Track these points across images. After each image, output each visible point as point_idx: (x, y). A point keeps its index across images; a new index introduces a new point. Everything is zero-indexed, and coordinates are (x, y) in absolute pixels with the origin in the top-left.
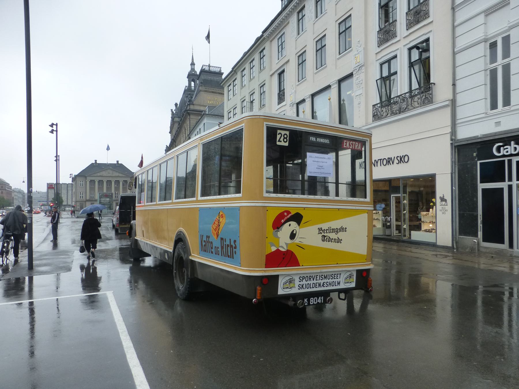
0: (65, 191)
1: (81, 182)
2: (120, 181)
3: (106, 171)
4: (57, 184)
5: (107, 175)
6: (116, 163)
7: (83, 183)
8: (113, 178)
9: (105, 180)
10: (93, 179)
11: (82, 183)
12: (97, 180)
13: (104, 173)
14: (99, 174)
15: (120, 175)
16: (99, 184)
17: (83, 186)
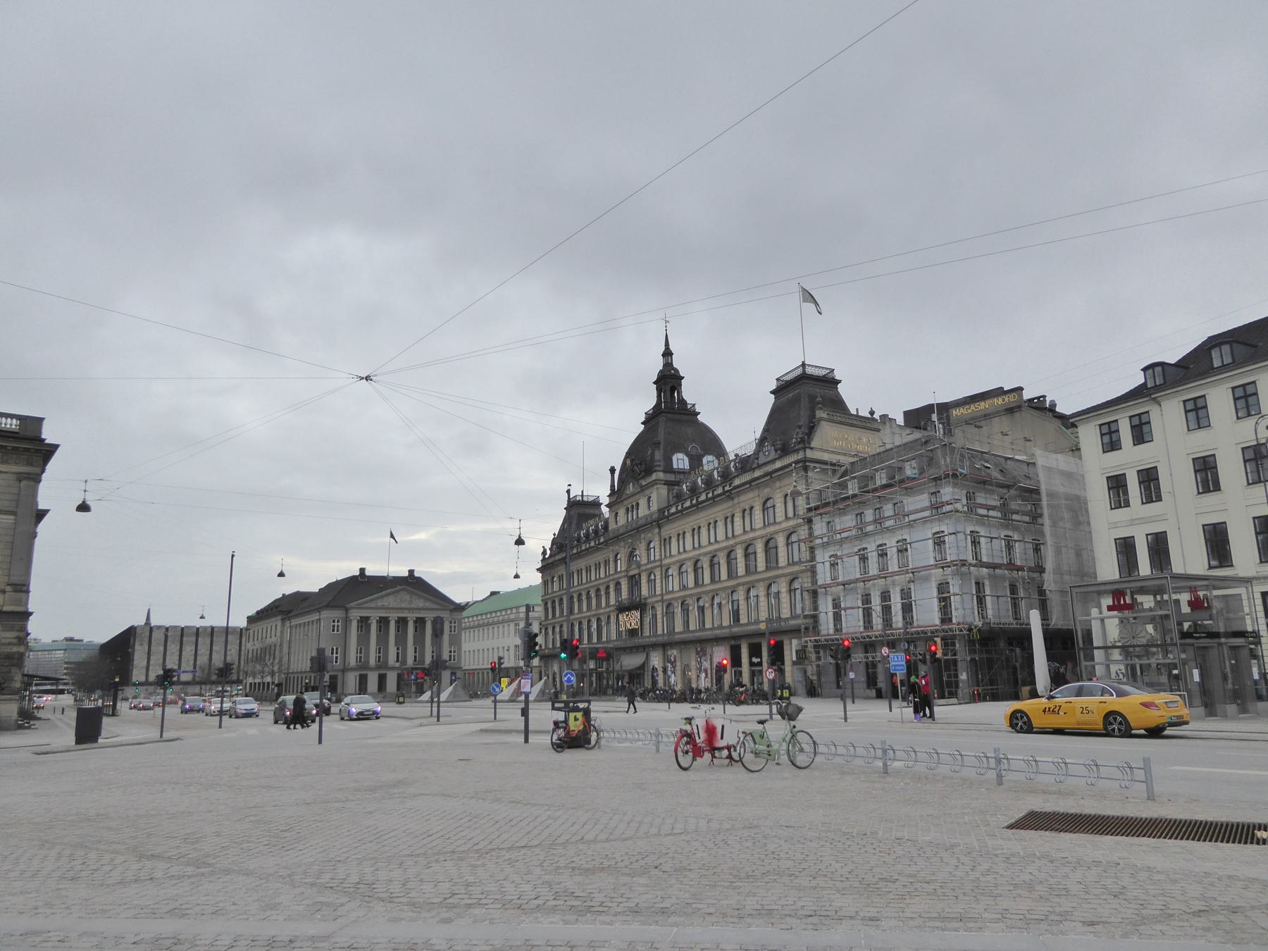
0: (177, 646)
1: (334, 621)
2: (390, 618)
3: (396, 595)
4: (227, 627)
5: (399, 606)
6: (407, 574)
7: (340, 624)
8: (388, 611)
9: (393, 616)
10: (365, 613)
11: (336, 624)
12: (374, 616)
13: (390, 601)
14: (380, 603)
15: (428, 605)
16: (362, 627)
17: (364, 632)
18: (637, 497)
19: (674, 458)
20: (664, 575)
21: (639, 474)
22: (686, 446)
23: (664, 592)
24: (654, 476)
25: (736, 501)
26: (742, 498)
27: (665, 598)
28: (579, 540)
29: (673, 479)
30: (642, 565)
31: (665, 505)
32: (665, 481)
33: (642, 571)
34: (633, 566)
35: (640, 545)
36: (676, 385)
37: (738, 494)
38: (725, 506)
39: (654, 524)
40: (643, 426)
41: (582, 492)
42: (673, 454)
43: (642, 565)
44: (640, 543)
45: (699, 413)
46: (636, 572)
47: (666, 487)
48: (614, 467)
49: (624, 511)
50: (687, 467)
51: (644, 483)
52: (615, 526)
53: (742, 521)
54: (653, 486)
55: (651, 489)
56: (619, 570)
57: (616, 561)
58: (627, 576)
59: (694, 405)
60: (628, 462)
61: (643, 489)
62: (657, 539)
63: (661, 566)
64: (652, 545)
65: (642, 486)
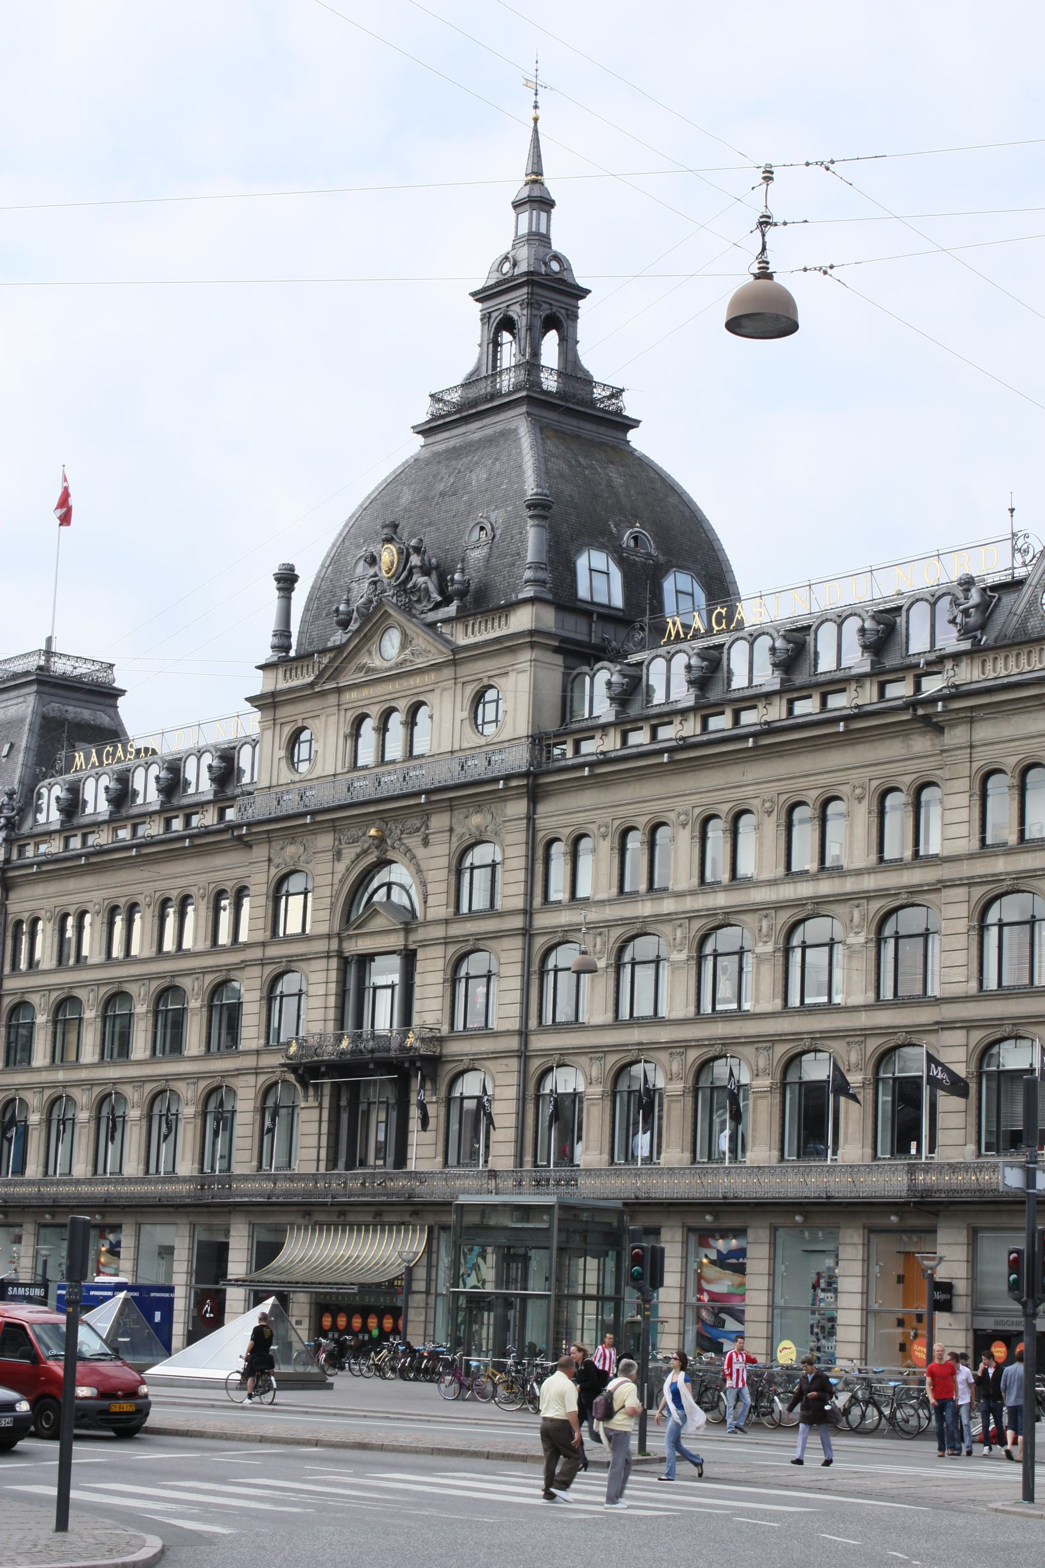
18: (417, 681)
19: (582, 563)
20: (535, 967)
21: (437, 606)
22: (614, 530)
23: (533, 1023)
24: (522, 620)
25: (956, 736)
26: (984, 731)
27: (538, 1042)
28: (72, 806)
29: (582, 637)
30: (426, 923)
31: (551, 724)
32: (564, 640)
33: (425, 944)
34: (379, 923)
35: (420, 852)
36: (562, 314)
37: (971, 715)
38: (893, 748)
39: (514, 783)
40: (420, 440)
41: (49, 640)
42: (579, 552)
43: (426, 923)
44: (426, 843)
45: (634, 424)
46: (396, 941)
47: (559, 660)
48: (291, 568)
49: (346, 728)
50: (618, 601)
51: (462, 639)
52: (286, 776)
53: (976, 803)
54: (512, 650)
55: (505, 660)
56: (294, 926)
57: (277, 893)
58: (340, 954)
59: (617, 393)
60: (388, 555)
61: (458, 657)
62: (517, 836)
63: (527, 933)
64: (481, 855)
65: (456, 650)
